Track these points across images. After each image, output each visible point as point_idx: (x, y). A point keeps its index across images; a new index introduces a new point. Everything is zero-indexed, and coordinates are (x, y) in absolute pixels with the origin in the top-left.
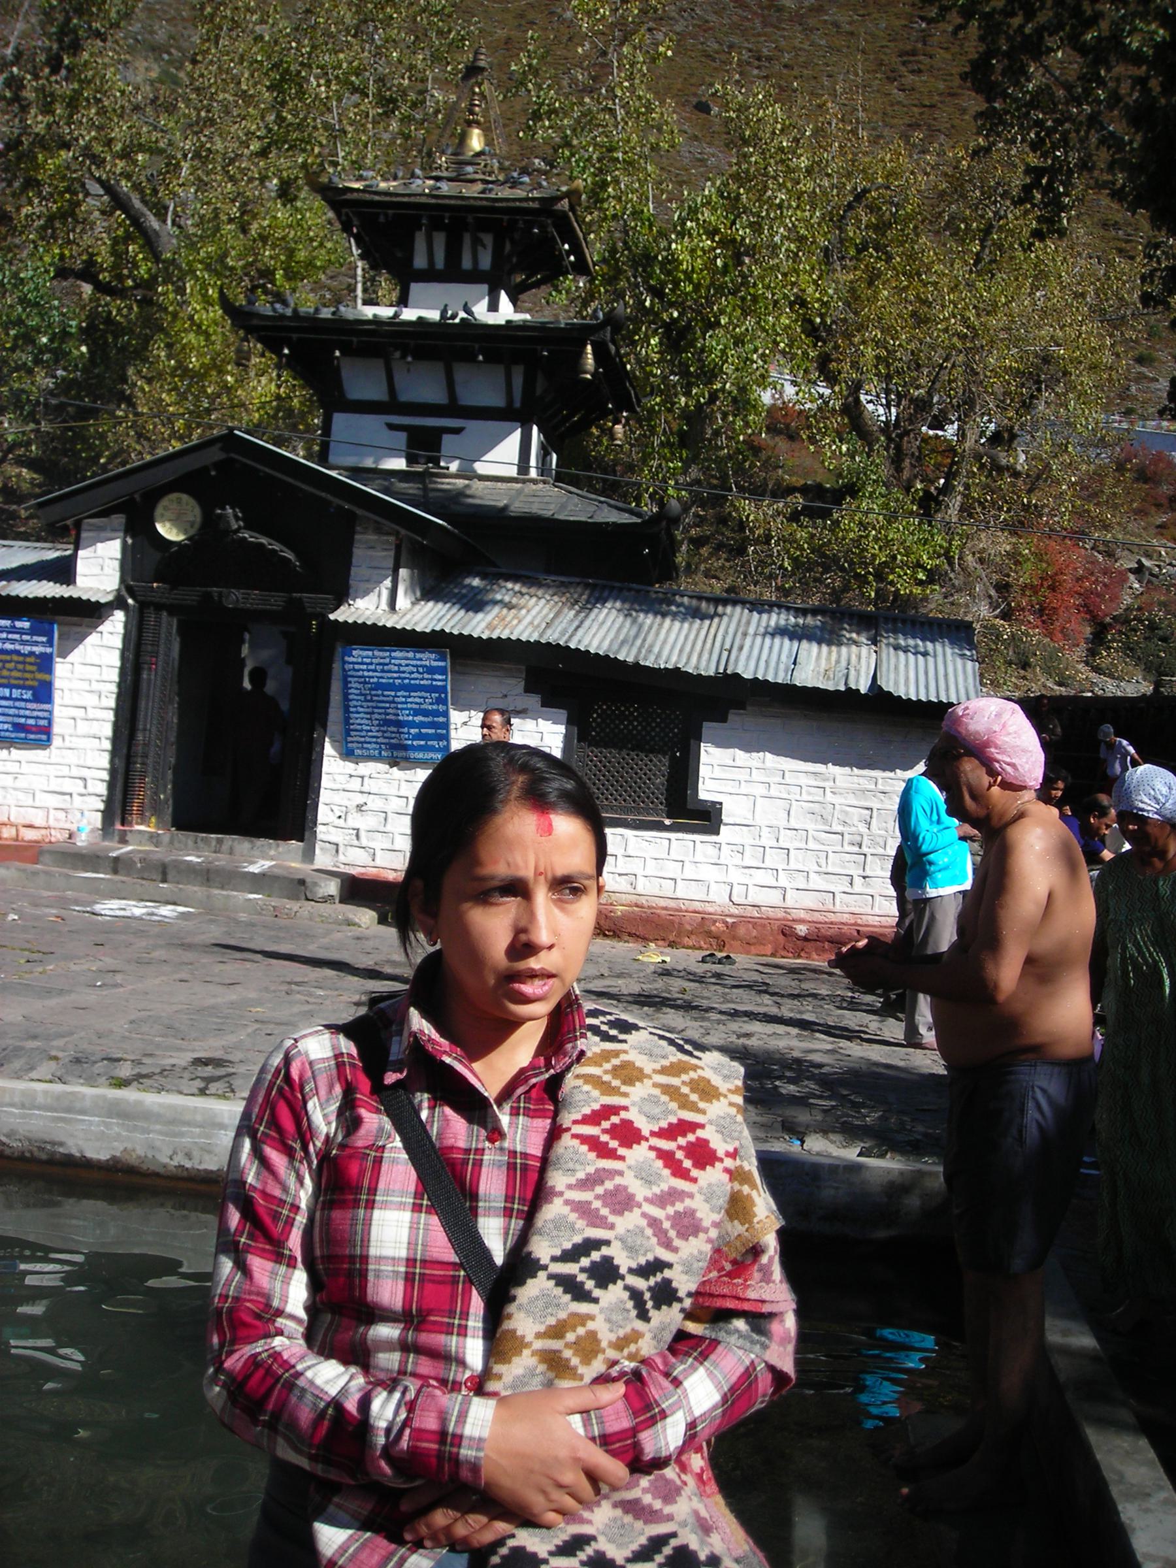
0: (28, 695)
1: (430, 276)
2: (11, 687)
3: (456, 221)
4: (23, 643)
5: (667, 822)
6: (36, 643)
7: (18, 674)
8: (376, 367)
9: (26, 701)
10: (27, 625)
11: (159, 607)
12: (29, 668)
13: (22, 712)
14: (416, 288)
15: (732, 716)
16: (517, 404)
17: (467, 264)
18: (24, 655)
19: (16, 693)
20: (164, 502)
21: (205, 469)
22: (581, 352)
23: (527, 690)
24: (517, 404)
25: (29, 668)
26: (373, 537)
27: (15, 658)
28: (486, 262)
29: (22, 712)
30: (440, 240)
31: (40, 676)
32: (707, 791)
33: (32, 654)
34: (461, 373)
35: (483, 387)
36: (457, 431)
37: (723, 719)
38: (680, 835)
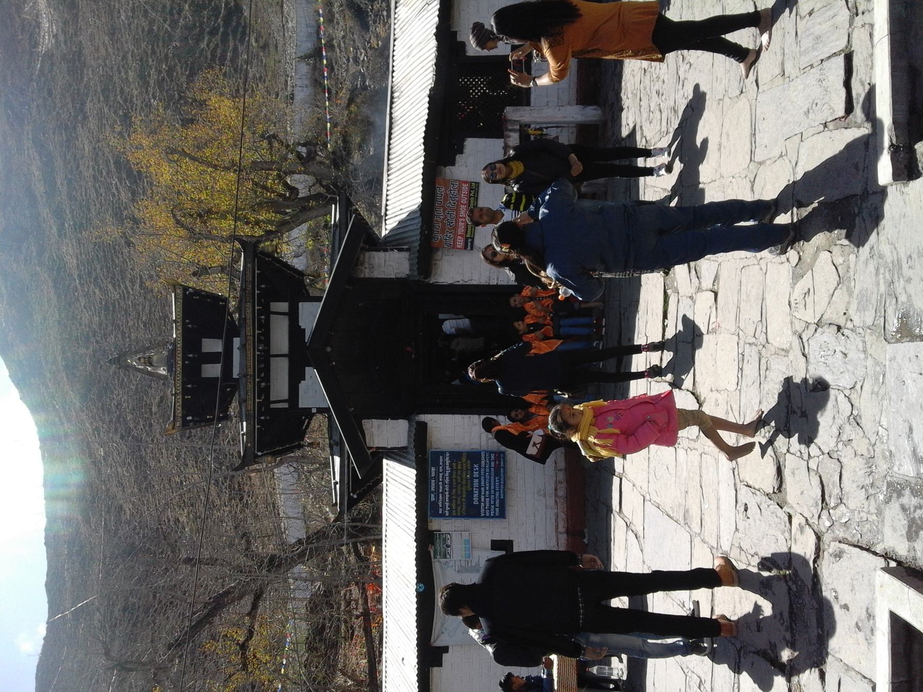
0: (476, 466)
2: (472, 478)
4: (444, 471)
6: (444, 462)
7: (464, 473)
9: (480, 467)
10: (433, 469)
12: (459, 467)
13: (488, 470)
18: (452, 470)
19: (476, 474)
25: (459, 467)
27: (454, 476)
29: (488, 470)
31: (464, 460)
33: (451, 466)
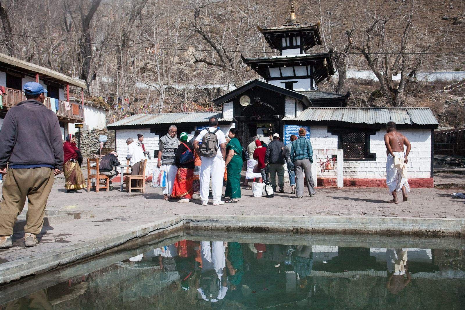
1: (287, 48)
3: (291, 34)
5: (364, 159)
8: (277, 70)
11: (242, 122)
14: (284, 51)
15: (377, 133)
16: (309, 74)
17: (294, 44)
20: (242, 98)
21: (251, 89)
22: (323, 61)
23: (328, 132)
24: (309, 74)
26: (289, 101)
28: (299, 44)
30: (288, 39)
32: (372, 151)
34: (296, 68)
35: (301, 71)
36: (296, 82)
37: (375, 134)
38: (367, 161)
